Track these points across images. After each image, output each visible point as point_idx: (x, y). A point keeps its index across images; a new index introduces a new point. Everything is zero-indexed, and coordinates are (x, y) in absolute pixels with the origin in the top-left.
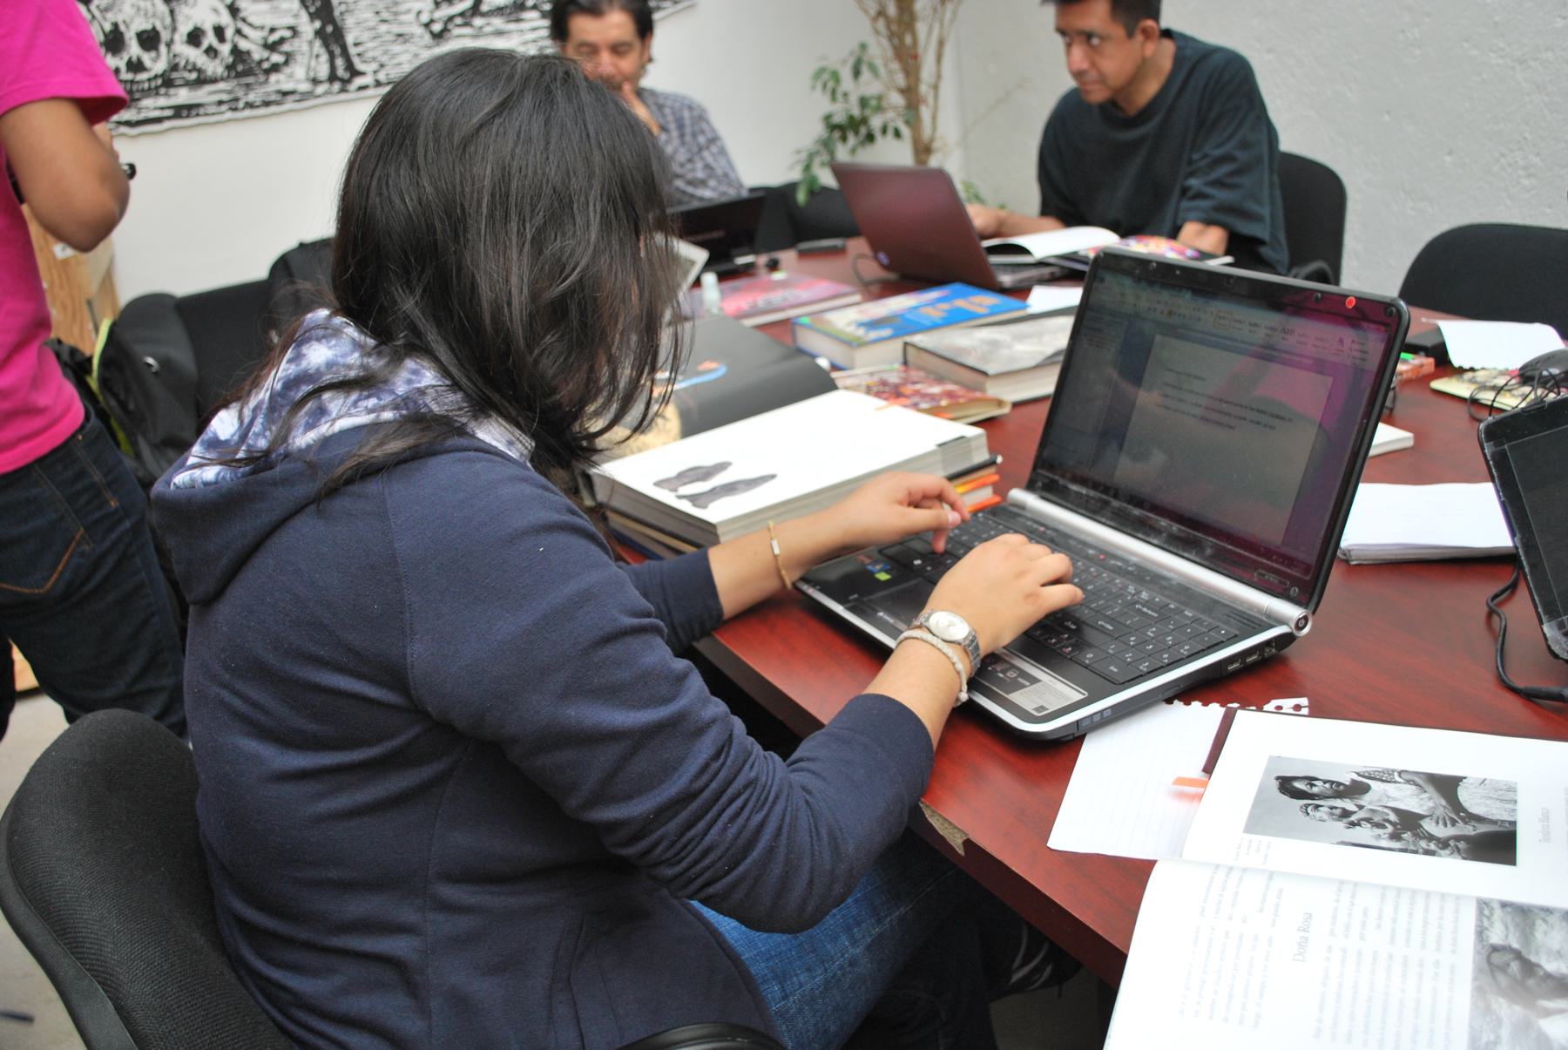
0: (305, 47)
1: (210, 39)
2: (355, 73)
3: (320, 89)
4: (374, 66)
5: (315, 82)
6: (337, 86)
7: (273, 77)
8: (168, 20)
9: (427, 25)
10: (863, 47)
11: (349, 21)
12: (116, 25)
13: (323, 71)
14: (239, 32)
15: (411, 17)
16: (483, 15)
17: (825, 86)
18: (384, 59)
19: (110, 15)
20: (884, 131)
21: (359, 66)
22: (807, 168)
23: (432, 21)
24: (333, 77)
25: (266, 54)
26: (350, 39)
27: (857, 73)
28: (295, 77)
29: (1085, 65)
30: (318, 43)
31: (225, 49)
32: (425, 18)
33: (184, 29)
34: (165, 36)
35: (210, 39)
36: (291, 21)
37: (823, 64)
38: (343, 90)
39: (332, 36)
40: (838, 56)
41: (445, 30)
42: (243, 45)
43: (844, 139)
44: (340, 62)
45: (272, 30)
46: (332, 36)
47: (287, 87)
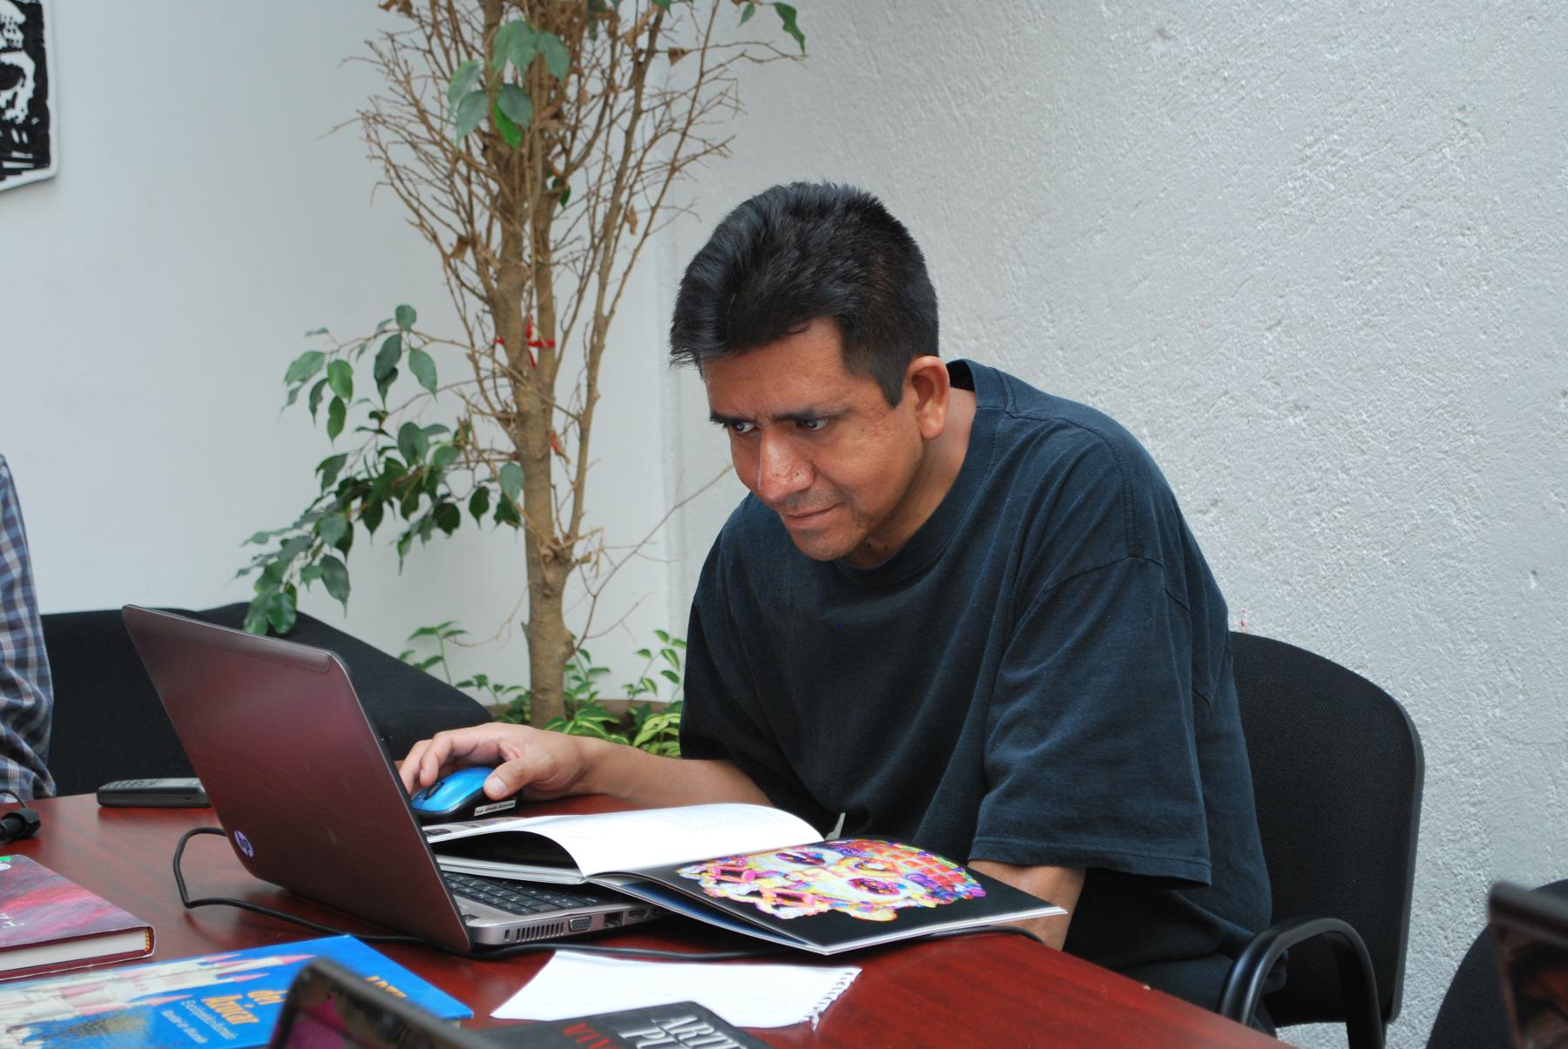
10: (405, 315)
17: (316, 395)
20: (478, 504)
22: (271, 575)
27: (385, 376)
37: (318, 344)
40: (353, 335)
43: (373, 518)
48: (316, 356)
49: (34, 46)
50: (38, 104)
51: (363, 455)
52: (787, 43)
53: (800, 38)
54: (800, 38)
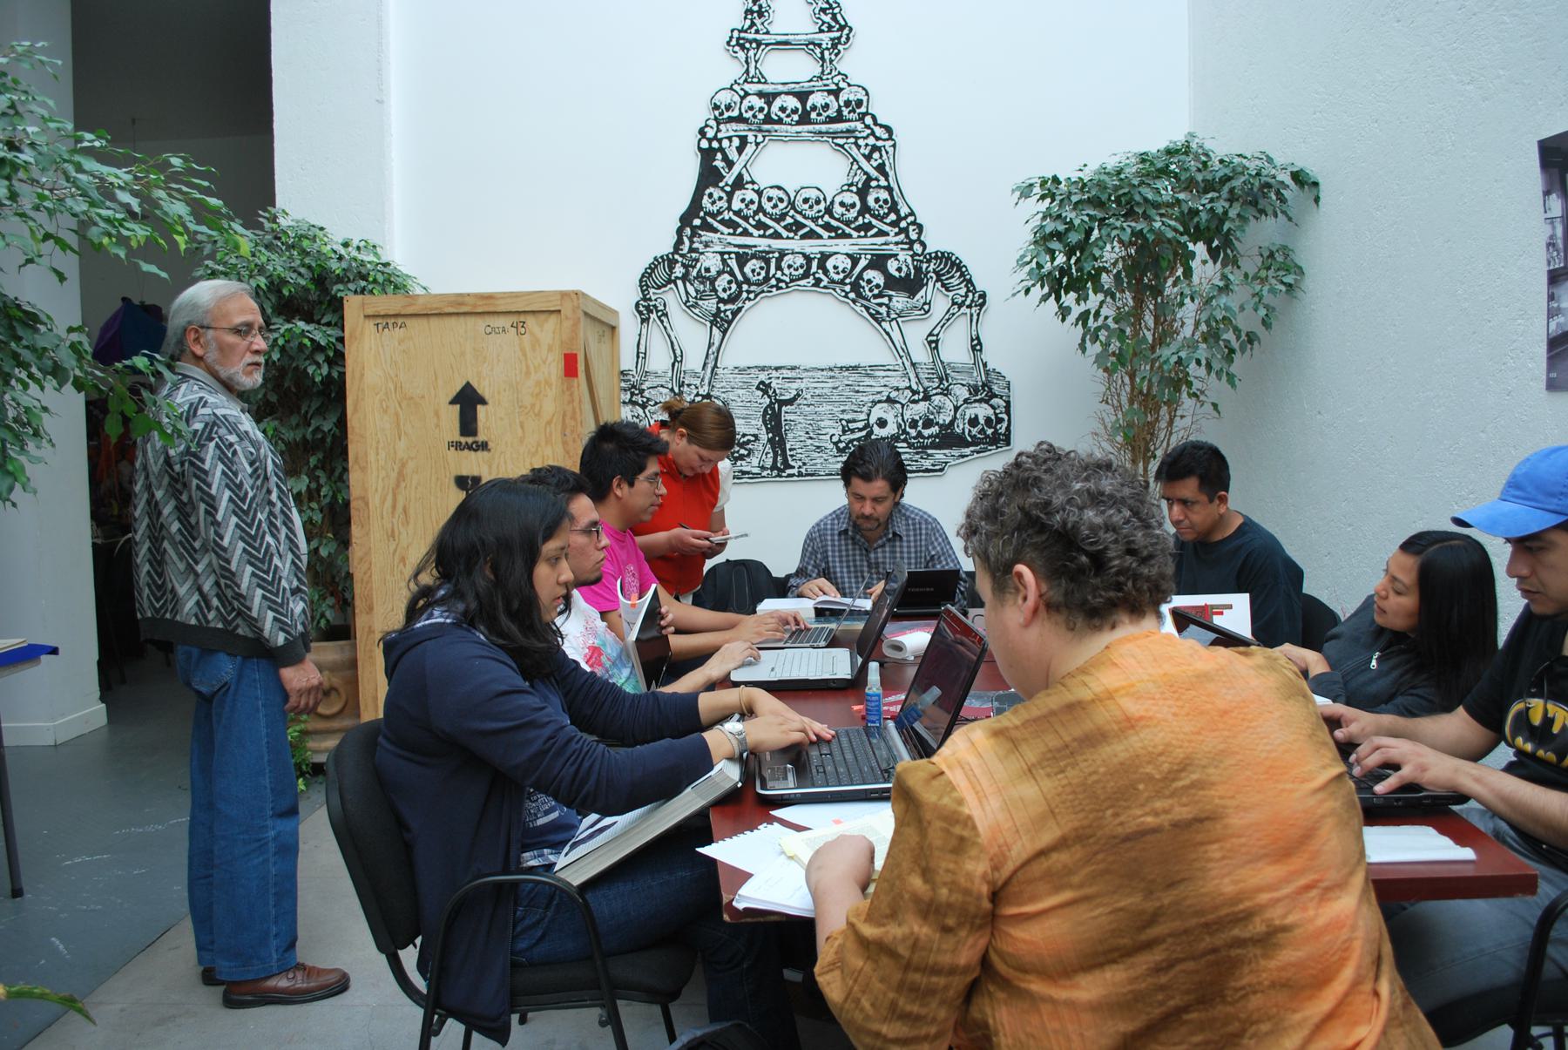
5: (763, 468)
9: (836, 444)
11: (790, 435)
13: (769, 462)
32: (835, 439)
39: (778, 442)
46: (778, 442)
49: (1008, 412)
50: (1008, 429)
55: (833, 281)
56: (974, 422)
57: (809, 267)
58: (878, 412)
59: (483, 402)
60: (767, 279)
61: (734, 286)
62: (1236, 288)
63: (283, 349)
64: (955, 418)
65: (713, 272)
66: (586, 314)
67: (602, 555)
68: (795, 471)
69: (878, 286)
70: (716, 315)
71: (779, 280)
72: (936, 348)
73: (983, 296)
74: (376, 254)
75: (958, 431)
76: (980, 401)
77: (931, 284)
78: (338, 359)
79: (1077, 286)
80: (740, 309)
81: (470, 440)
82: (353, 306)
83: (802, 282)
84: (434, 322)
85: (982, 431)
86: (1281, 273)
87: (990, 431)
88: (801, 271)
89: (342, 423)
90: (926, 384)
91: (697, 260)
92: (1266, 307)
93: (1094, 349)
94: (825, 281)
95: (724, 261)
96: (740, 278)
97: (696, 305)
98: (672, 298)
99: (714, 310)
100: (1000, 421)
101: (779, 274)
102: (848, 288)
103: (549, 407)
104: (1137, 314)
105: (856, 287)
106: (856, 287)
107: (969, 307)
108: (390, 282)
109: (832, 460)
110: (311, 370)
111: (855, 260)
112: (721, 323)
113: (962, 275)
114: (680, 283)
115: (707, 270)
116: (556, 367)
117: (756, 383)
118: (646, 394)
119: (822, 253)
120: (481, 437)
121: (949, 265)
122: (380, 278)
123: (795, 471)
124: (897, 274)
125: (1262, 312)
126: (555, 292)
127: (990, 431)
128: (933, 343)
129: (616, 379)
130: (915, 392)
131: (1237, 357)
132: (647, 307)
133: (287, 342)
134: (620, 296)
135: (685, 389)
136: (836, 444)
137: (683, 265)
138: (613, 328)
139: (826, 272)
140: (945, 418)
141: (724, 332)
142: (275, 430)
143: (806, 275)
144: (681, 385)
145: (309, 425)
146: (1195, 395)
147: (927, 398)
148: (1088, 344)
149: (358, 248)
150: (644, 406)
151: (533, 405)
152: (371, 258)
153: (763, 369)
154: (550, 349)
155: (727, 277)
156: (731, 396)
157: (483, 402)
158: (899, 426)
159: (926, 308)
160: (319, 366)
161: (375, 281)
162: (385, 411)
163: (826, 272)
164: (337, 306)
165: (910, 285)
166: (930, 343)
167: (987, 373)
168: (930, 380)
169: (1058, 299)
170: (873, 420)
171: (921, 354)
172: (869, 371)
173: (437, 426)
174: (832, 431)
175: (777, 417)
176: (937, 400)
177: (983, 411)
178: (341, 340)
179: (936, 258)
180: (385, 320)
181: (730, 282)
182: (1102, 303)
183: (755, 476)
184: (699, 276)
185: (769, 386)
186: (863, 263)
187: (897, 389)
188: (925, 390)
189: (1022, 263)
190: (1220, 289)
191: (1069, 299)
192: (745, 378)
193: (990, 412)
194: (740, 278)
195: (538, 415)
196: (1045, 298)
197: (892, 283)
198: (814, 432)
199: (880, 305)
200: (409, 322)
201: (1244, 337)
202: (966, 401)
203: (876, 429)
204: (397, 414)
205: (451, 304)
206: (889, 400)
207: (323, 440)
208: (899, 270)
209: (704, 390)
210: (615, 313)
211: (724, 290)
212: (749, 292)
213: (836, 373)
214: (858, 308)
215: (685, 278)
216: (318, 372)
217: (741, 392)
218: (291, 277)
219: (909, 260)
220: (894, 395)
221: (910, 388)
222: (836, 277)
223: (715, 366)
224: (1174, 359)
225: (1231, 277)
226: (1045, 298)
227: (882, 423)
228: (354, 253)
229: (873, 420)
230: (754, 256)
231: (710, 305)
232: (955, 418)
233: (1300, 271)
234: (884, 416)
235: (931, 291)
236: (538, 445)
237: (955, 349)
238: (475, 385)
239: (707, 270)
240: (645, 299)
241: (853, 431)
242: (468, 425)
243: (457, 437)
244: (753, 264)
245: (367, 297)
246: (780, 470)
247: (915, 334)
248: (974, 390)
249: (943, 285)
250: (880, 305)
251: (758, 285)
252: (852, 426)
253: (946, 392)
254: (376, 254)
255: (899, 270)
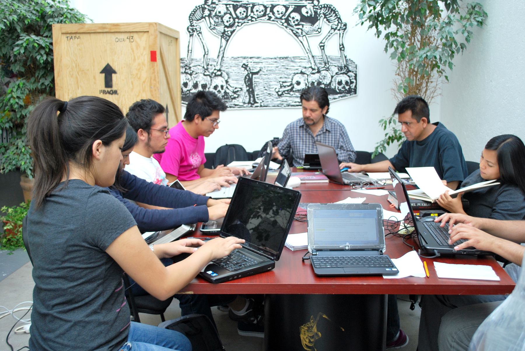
0: (243, 94)
1: (219, 88)
2: (255, 102)
3: (245, 105)
4: (261, 101)
5: (244, 103)
6: (250, 105)
7: (234, 100)
8: (210, 82)
9: (277, 92)
11: (256, 88)
12: (197, 82)
13: (247, 101)
14: (227, 87)
15: (274, 89)
16: (293, 92)
18: (264, 100)
19: (196, 79)
21: (257, 101)
23: (279, 91)
24: (249, 103)
25: (233, 94)
26: (256, 93)
27: (390, 122)
28: (239, 101)
29: (406, 130)
30: (247, 93)
31: (223, 91)
32: (277, 90)
33: (214, 85)
34: (208, 86)
35: (219, 88)
36: (241, 87)
37: (383, 118)
38: (251, 107)
39: (251, 92)
41: (282, 94)
42: (228, 91)
43: (392, 142)
44: (252, 99)
45: (236, 88)
46: (251, 92)
47: (236, 103)
48: (383, 120)
49: (356, 79)
50: (356, 86)
51: (391, 133)
52: (446, 81)
53: (448, 80)
54: (448, 80)
55: (277, 18)
56: (340, 83)
57: (266, 11)
58: (297, 78)
59: (115, 72)
60: (247, 17)
61: (232, 20)
62: (454, 23)
63: (26, 48)
64: (331, 81)
65: (222, 14)
66: (161, 33)
67: (166, 141)
68: (258, 105)
69: (297, 20)
70: (223, 33)
71: (252, 17)
72: (323, 49)
73: (345, 25)
74: (67, 5)
75: (333, 87)
76: (343, 73)
77: (321, 19)
78: (50, 52)
79: (386, 22)
80: (234, 31)
81: (109, 89)
82: (56, 28)
83: (263, 18)
84: (93, 36)
85: (344, 87)
86: (476, 16)
87: (347, 88)
88: (262, 13)
89: (53, 81)
90: (319, 65)
91: (215, 8)
92: (468, 32)
93: (391, 50)
94: (273, 18)
95: (227, 8)
96: (234, 16)
97: (214, 29)
98: (203, 25)
99: (223, 31)
100: (352, 83)
101: (252, 15)
102: (283, 21)
103: (144, 74)
104: (413, 33)
105: (287, 20)
106: (287, 20)
107: (339, 30)
108: (75, 18)
109: (275, 100)
110: (38, 57)
111: (287, 9)
112: (226, 36)
113: (336, 15)
114: (207, 18)
115: (220, 12)
116: (147, 57)
117: (242, 64)
118: (192, 69)
119: (272, 5)
120: (114, 88)
121: (331, 10)
122: (69, 16)
123: (258, 105)
124: (306, 15)
125: (466, 34)
126: (146, 23)
127: (347, 88)
128: (322, 47)
129: (178, 62)
130: (313, 69)
131: (455, 54)
132: (192, 29)
133: (28, 44)
134: (180, 24)
135: (209, 67)
136: (277, 92)
137: (209, 10)
138: (177, 39)
139: (273, 14)
140: (327, 81)
141: (227, 41)
142: (24, 84)
143: (264, 15)
144: (208, 65)
145: (39, 82)
146: (440, 72)
147: (319, 72)
148: (388, 48)
149: (59, 2)
150: (191, 74)
151: (137, 74)
152: (65, 6)
153: (245, 58)
154: (144, 49)
155: (228, 16)
156: (230, 70)
157: (115, 72)
158: (306, 85)
159: (319, 31)
160: (42, 55)
161: (67, 17)
162: (72, 76)
163: (273, 14)
164: (49, 28)
165: (312, 20)
166: (321, 46)
167: (347, 61)
168: (320, 63)
169: (377, 27)
170: (294, 82)
171: (317, 52)
172: (293, 60)
173: (95, 83)
174: (275, 87)
175: (250, 80)
176: (323, 73)
177: (344, 78)
178: (51, 44)
179: (324, 7)
180: (71, 35)
181: (230, 18)
182: (398, 29)
183: (241, 106)
184: (216, 15)
185: (247, 66)
186: (291, 9)
187: (305, 68)
188: (318, 69)
189: (355, 10)
190: (447, 24)
191: (381, 27)
192: (236, 62)
193: (347, 79)
194: (234, 16)
195: (139, 78)
196: (371, 27)
197: (304, 19)
198: (267, 87)
199: (298, 29)
200: (82, 36)
201: (459, 46)
202: (336, 74)
203: (295, 86)
204: (77, 78)
205: (100, 28)
206: (302, 73)
207: (46, 88)
208: (307, 13)
209: (218, 68)
210: (178, 32)
211: (227, 22)
212: (238, 23)
213: (278, 60)
214: (288, 30)
215: (209, 16)
216: (42, 58)
217: (234, 68)
218: (29, 15)
219: (312, 8)
220: (304, 70)
221: (311, 67)
222: (279, 16)
223: (223, 57)
224: (425, 55)
225: (452, 18)
226: (371, 27)
227: (298, 83)
228: (58, 5)
229: (294, 82)
230: (241, 6)
231: (221, 28)
232: (331, 81)
233: (485, 15)
234: (299, 80)
235: (322, 23)
236: (140, 92)
237: (332, 50)
238: (111, 65)
239: (220, 12)
240: (191, 26)
241: (285, 87)
242: (108, 83)
243: (103, 88)
244: (241, 10)
245: (63, 25)
246: (252, 104)
247: (314, 42)
248: (341, 68)
249: (327, 20)
250: (298, 29)
251: (243, 19)
252: (284, 84)
253: (328, 69)
254: (67, 5)
255: (307, 13)
